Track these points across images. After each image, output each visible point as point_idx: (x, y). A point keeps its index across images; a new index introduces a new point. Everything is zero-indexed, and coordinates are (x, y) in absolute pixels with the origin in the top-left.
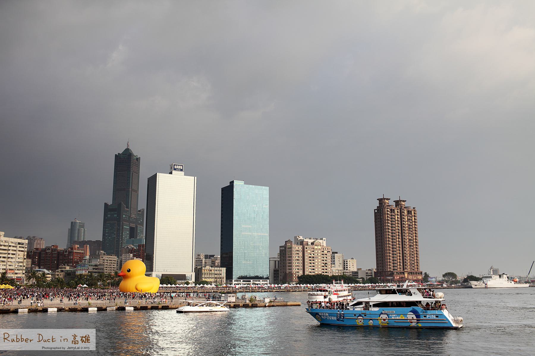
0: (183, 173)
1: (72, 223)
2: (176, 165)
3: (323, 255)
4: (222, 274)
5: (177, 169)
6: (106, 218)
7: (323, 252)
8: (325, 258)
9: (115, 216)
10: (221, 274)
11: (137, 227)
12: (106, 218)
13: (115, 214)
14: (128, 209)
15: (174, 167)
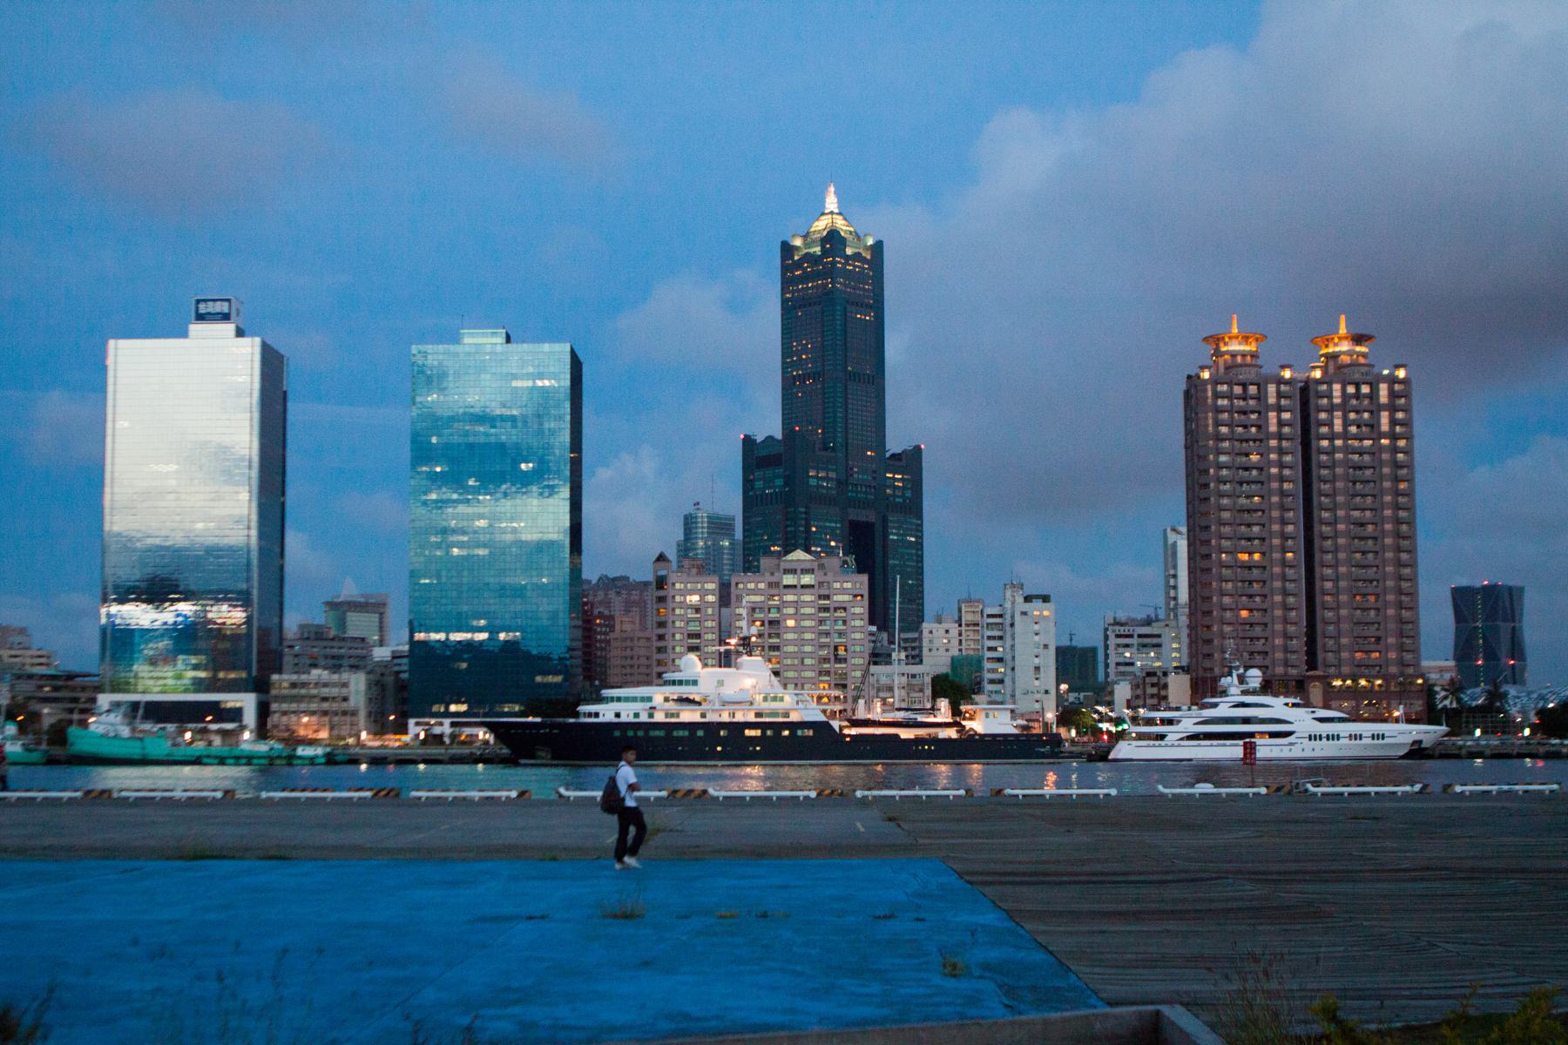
0: (230, 328)
1: (686, 517)
2: (205, 301)
3: (826, 609)
4: (352, 703)
5: (209, 314)
6: (751, 493)
7: (827, 597)
8: (840, 626)
9: (779, 482)
10: (345, 699)
11: (885, 520)
12: (751, 493)
13: (778, 477)
14: (833, 454)
15: (197, 308)
